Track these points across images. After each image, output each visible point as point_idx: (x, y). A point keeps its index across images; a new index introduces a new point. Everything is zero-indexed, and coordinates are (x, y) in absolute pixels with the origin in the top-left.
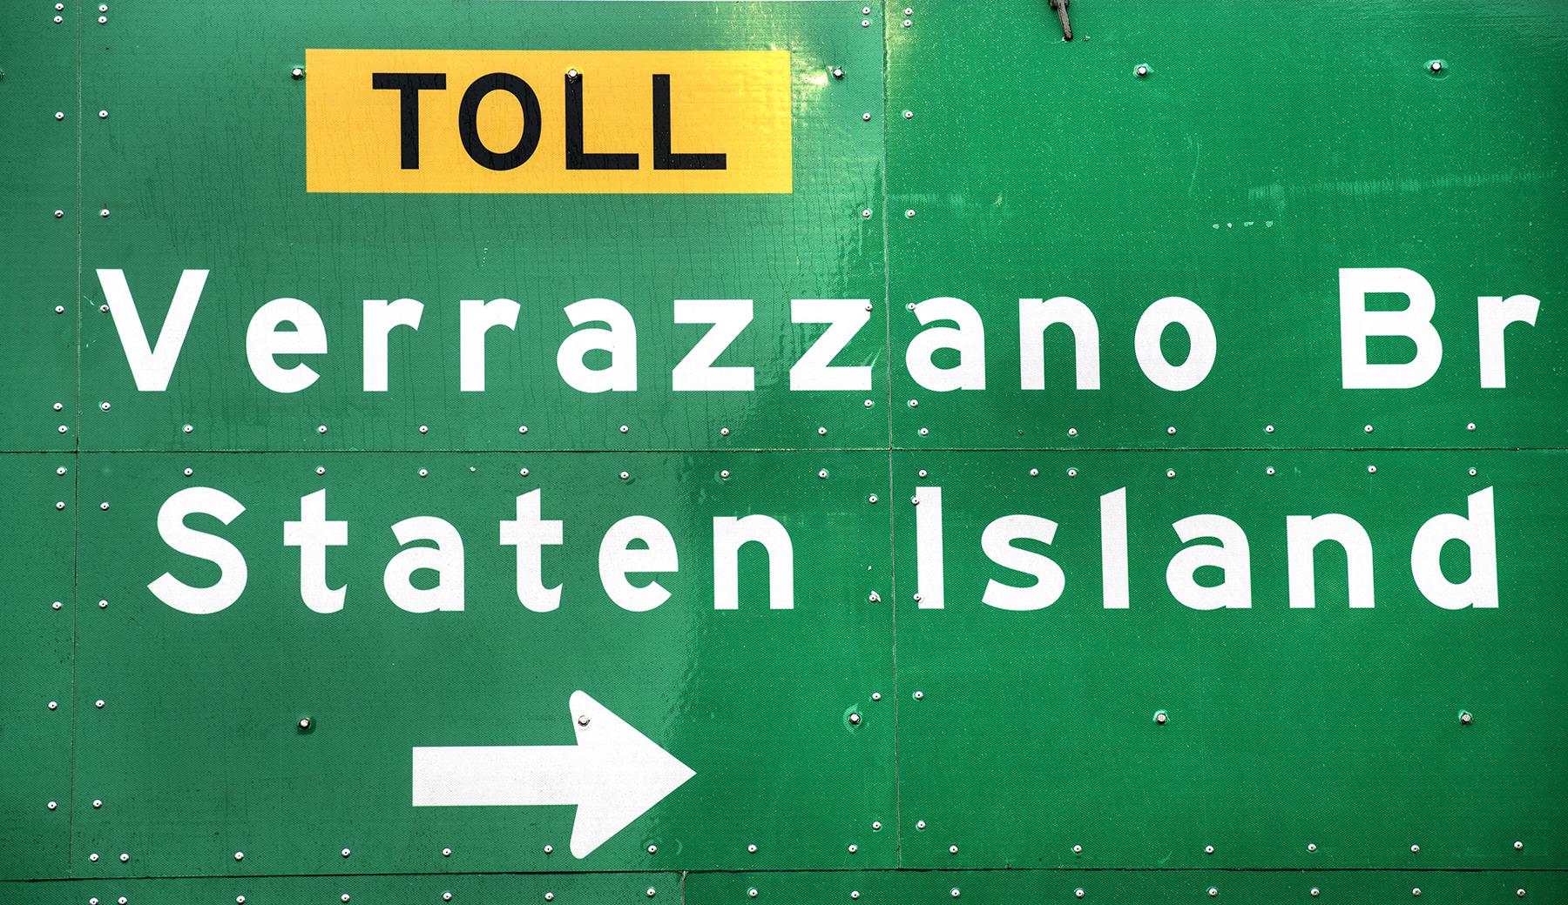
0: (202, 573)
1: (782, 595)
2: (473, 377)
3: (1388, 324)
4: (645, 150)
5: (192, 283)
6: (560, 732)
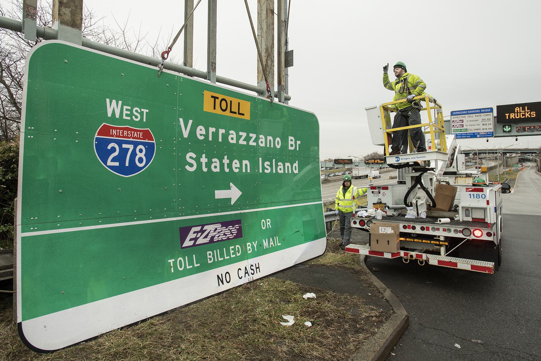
4: (237, 113)
5: (191, 122)
6: (229, 188)
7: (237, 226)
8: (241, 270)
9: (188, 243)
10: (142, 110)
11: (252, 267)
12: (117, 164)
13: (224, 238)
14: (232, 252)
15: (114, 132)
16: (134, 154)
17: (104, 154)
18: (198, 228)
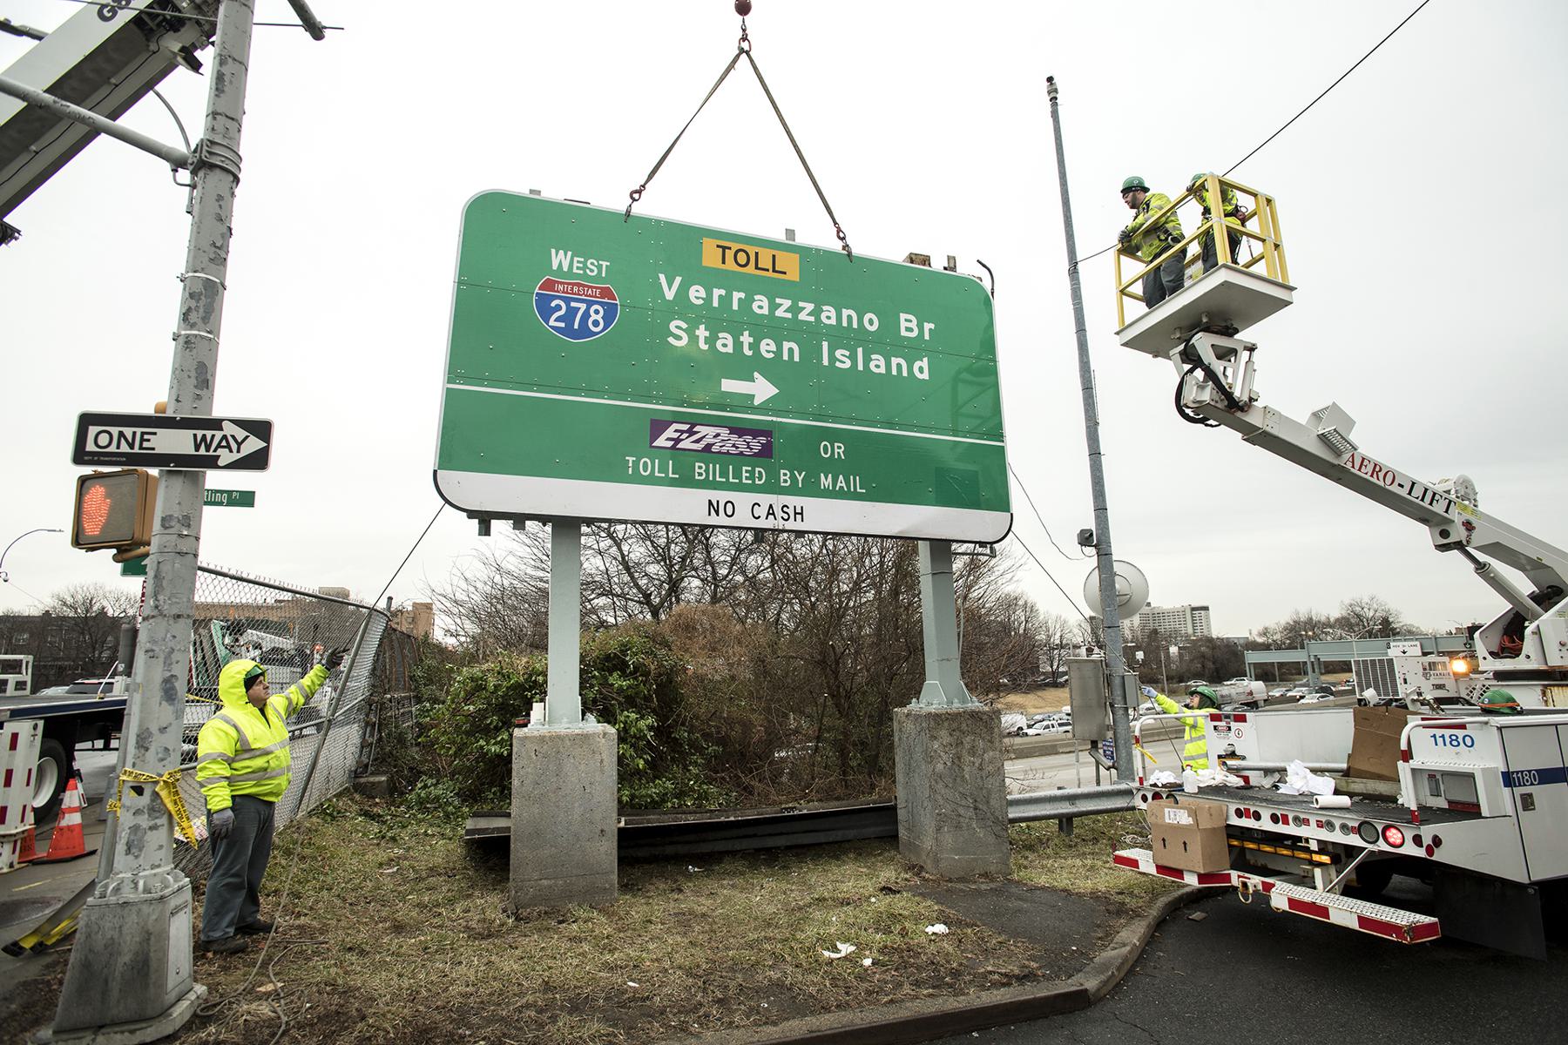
0: (679, 338)
1: (797, 359)
2: (735, 307)
3: (909, 325)
4: (771, 270)
5: (678, 279)
7: (763, 440)
8: (759, 506)
9: (661, 442)
10: (600, 262)
11: (785, 509)
12: (562, 325)
13: (733, 450)
14: (744, 474)
15: (561, 287)
16: (586, 315)
17: (546, 312)
18: (686, 427)
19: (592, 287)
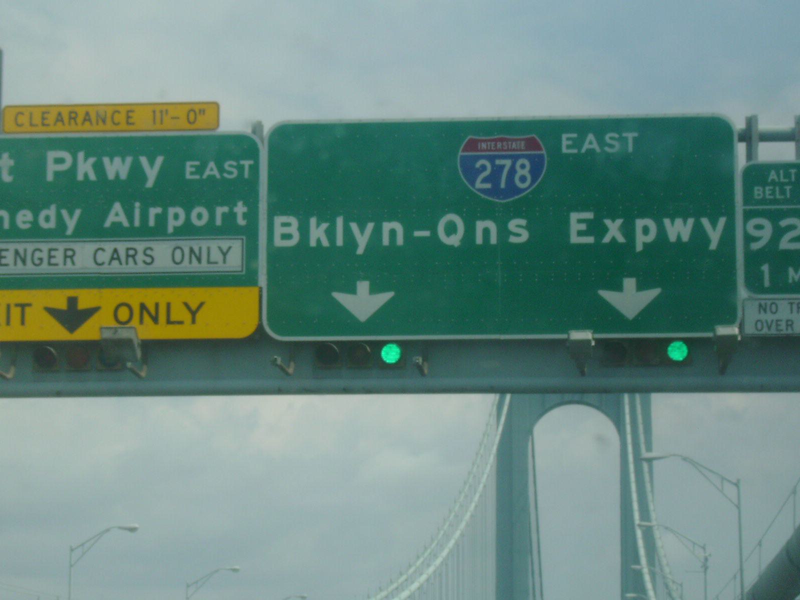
12: (488, 186)
15: (484, 146)
16: (512, 171)
17: (471, 173)
19: (516, 140)
